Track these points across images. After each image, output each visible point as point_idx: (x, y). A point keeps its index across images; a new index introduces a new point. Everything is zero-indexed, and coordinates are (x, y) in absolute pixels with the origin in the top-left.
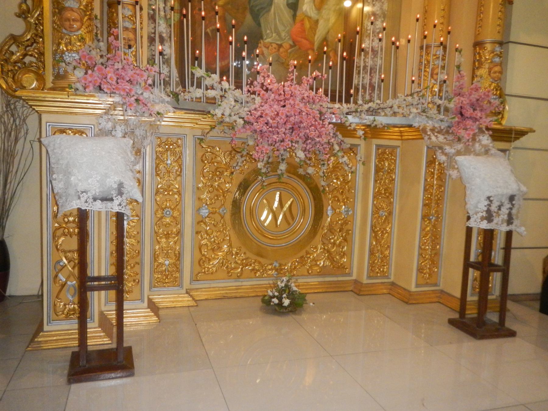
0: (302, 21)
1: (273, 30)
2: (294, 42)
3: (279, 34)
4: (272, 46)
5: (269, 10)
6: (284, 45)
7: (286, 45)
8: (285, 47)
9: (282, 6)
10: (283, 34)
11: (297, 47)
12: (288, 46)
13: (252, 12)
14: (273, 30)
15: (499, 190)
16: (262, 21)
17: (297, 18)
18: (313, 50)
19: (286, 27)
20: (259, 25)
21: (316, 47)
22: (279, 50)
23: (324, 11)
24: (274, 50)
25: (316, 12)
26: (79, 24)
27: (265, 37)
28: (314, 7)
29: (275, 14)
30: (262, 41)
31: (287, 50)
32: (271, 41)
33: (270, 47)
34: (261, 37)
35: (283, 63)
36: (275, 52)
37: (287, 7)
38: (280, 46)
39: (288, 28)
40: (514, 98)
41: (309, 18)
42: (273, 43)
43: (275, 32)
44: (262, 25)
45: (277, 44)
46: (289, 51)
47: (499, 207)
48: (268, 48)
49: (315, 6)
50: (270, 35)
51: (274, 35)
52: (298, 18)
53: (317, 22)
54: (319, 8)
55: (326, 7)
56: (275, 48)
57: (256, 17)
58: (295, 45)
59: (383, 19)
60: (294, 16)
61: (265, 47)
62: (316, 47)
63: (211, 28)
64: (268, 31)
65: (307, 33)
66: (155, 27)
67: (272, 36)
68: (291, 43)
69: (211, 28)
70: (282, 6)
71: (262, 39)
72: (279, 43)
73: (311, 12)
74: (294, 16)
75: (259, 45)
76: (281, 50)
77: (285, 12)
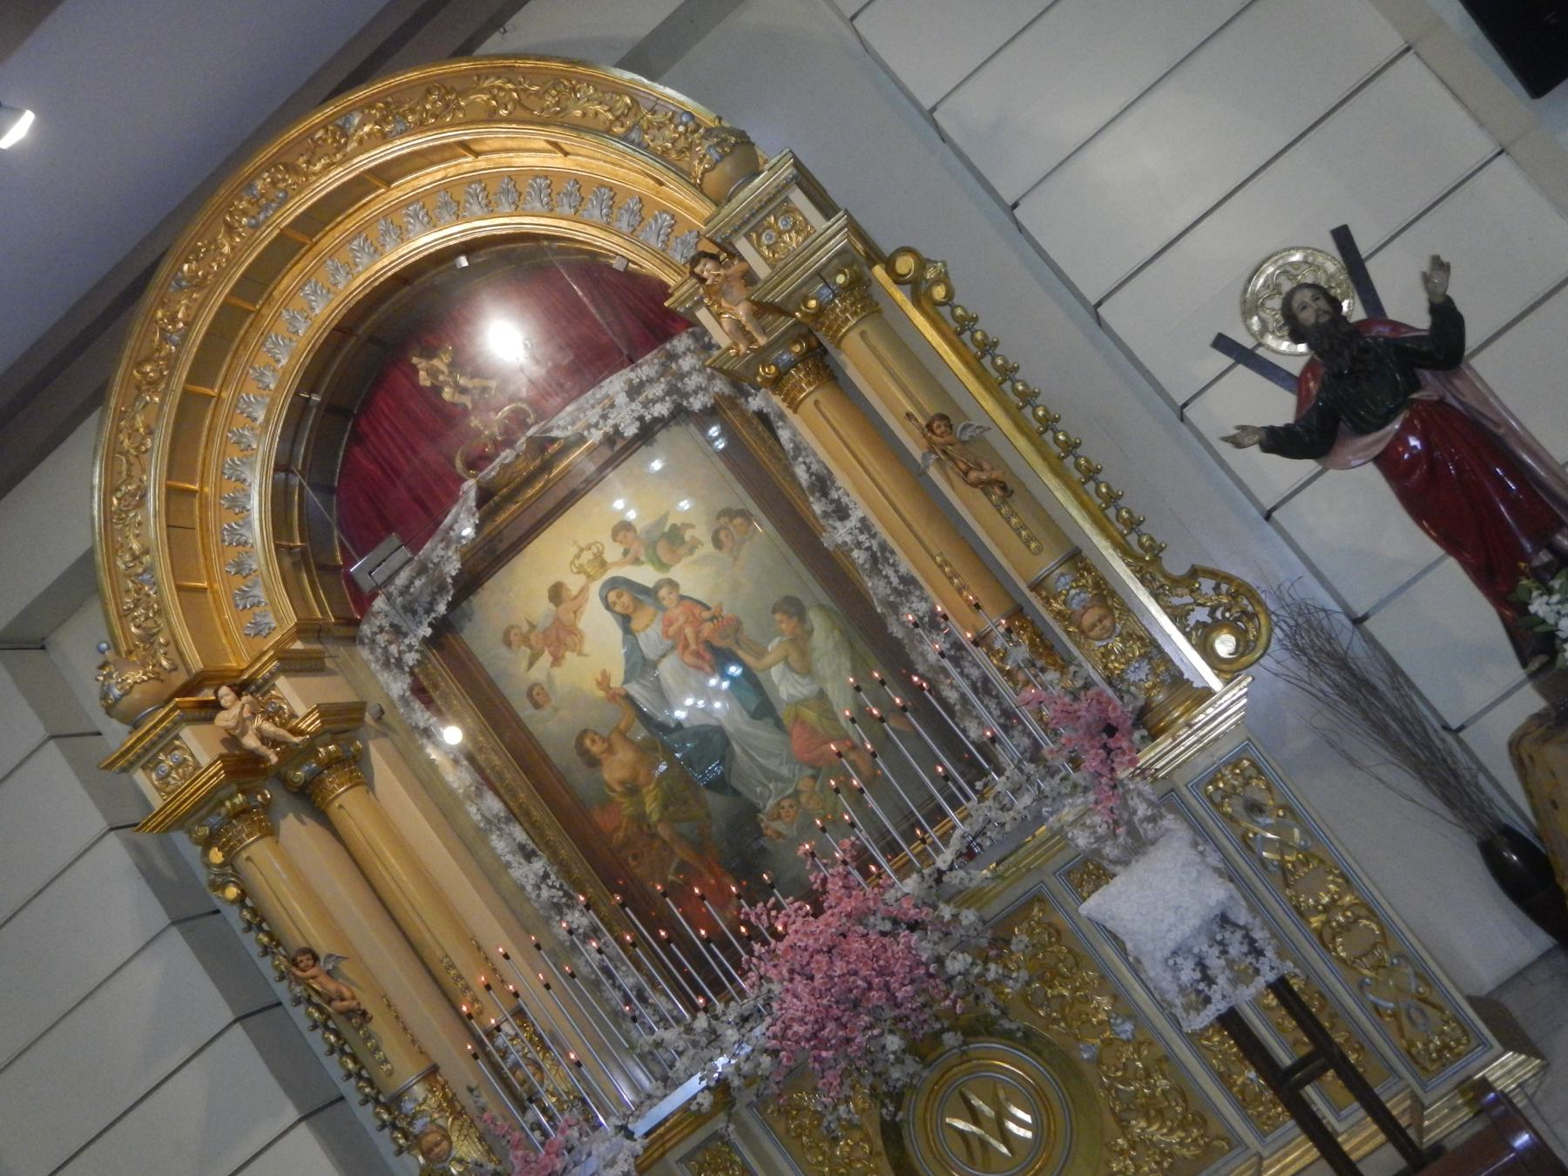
0: (797, 717)
1: (763, 780)
2: (812, 767)
3: (777, 778)
5: (733, 753)
6: (801, 786)
7: (804, 784)
10: (785, 771)
12: (810, 783)
14: (763, 780)
15: (1171, 935)
16: (735, 782)
20: (736, 793)
22: (799, 803)
25: (806, 681)
26: (445, 1144)
28: (796, 677)
30: (761, 816)
33: (783, 813)
34: (753, 811)
37: (757, 722)
39: (785, 754)
40: (1293, 500)
41: (803, 702)
43: (770, 780)
45: (788, 797)
47: (1201, 965)
48: (779, 817)
50: (767, 792)
51: (771, 786)
53: (822, 695)
54: (807, 671)
55: (816, 655)
56: (791, 806)
58: (819, 770)
59: (918, 593)
60: (778, 724)
61: (774, 820)
64: (758, 790)
65: (821, 731)
66: (587, 961)
68: (809, 772)
71: (759, 811)
72: (790, 791)
73: (799, 688)
74: (778, 724)
75: (763, 825)
76: (803, 799)
77: (760, 733)
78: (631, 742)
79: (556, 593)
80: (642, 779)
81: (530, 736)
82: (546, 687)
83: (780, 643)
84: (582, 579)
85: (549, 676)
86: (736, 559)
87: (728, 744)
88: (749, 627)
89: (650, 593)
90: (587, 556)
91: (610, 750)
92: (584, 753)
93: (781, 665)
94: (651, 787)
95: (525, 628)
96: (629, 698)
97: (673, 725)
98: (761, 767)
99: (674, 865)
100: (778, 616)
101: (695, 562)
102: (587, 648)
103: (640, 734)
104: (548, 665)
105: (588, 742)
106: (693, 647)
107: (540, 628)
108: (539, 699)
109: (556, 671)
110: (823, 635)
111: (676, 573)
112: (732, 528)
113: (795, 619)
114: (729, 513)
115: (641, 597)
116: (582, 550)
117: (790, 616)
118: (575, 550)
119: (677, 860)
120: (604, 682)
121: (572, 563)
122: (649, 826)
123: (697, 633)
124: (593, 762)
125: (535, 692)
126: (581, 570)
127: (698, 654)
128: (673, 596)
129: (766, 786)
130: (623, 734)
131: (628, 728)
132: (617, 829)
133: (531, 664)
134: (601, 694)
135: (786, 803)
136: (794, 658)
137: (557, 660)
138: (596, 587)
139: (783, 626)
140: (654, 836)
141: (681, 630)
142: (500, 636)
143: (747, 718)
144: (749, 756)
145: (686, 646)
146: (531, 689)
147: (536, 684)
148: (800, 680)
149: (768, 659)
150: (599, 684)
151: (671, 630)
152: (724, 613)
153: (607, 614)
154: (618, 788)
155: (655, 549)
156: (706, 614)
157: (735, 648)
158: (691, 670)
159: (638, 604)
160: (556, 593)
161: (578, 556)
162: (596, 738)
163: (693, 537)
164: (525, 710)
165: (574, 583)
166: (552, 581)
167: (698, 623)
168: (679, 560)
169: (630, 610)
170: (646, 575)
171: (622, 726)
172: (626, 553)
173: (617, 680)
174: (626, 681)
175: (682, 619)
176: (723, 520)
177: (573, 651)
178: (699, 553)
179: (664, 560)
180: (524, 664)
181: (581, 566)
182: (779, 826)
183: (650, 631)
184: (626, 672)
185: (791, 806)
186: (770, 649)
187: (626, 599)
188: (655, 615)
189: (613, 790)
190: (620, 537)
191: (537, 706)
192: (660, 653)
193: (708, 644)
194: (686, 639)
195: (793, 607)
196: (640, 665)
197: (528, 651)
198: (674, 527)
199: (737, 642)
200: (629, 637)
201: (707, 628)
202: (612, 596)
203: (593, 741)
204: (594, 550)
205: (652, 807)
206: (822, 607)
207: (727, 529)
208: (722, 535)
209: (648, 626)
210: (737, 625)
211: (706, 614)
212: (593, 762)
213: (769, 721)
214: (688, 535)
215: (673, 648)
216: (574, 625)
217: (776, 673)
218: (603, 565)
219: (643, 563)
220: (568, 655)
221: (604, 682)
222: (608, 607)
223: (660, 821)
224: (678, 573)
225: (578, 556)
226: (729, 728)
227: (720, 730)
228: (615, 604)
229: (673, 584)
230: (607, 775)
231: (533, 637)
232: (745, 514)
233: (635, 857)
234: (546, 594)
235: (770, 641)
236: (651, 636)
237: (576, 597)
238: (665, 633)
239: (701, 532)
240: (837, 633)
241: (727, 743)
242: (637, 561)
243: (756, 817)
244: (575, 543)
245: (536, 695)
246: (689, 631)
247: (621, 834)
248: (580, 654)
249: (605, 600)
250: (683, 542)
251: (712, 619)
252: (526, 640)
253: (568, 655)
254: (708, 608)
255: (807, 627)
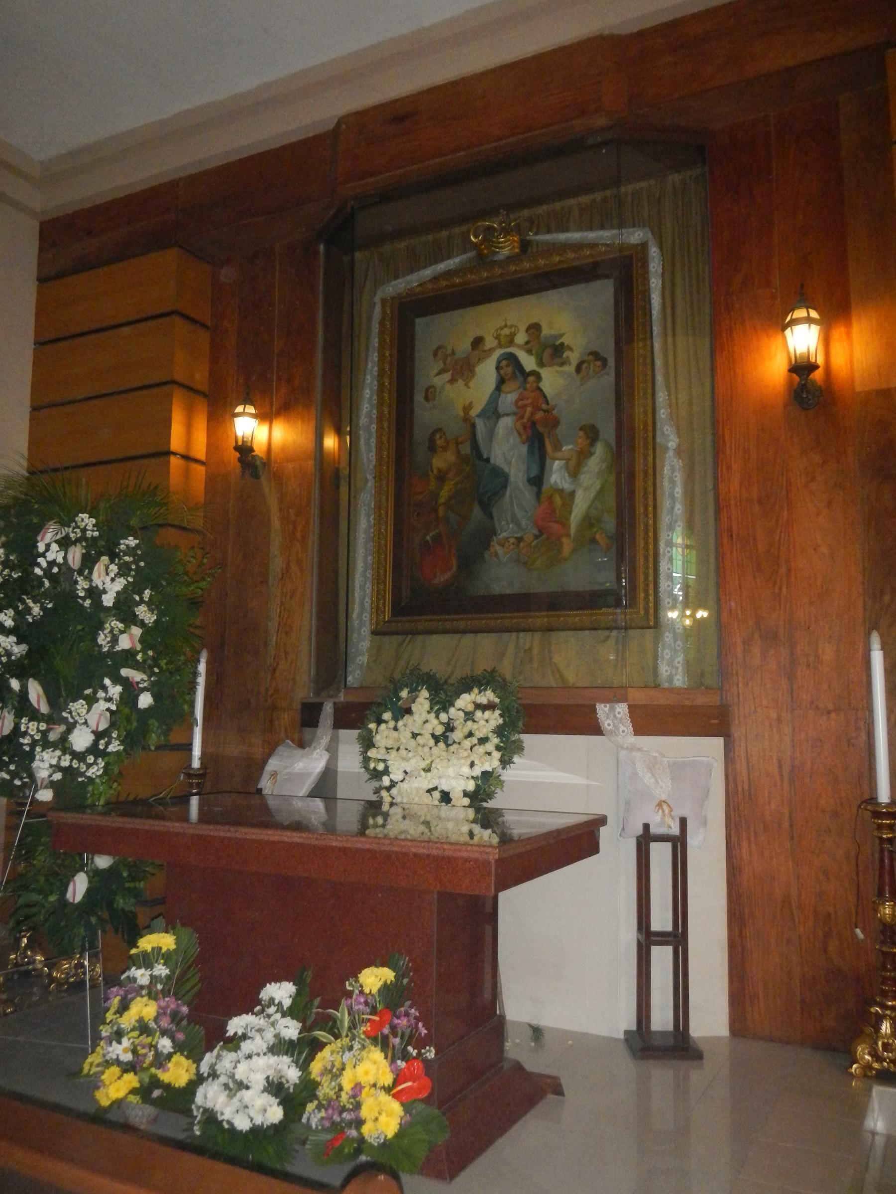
0: (550, 499)
1: (510, 521)
2: (539, 531)
3: (517, 524)
4: (508, 542)
5: (504, 495)
6: (525, 537)
7: (528, 538)
8: (527, 540)
9: (521, 485)
10: (524, 523)
11: (544, 536)
12: (532, 538)
13: (480, 502)
17: (542, 496)
18: (568, 535)
19: (526, 511)
20: (491, 517)
21: (573, 531)
22: (518, 546)
23: (583, 477)
24: (512, 547)
27: (499, 532)
28: (567, 474)
29: (511, 496)
30: (495, 538)
31: (529, 545)
32: (508, 536)
34: (494, 533)
35: (525, 564)
36: (513, 549)
38: (520, 540)
41: (561, 491)
42: (509, 537)
43: (512, 522)
44: (495, 519)
45: (517, 538)
46: (533, 544)
48: (503, 546)
49: (568, 472)
51: (511, 526)
52: (544, 496)
53: (572, 494)
54: (574, 473)
55: (586, 469)
56: (513, 544)
57: (486, 508)
60: (538, 494)
61: (499, 545)
62: (573, 531)
63: (431, 535)
64: (503, 523)
65: (558, 513)
67: (508, 527)
68: (535, 532)
69: (431, 535)
70: (521, 485)
71: (495, 534)
72: (518, 535)
73: (563, 482)
75: (492, 544)
76: (522, 544)
78: (458, 451)
79: (478, 342)
80: (450, 475)
81: (412, 412)
82: (438, 391)
83: (571, 449)
84: (496, 343)
85: (443, 387)
86: (582, 385)
87: (505, 487)
88: (561, 430)
89: (525, 375)
90: (506, 331)
91: (445, 449)
92: (432, 440)
93: (563, 462)
94: (452, 482)
95: (449, 352)
96: (473, 426)
97: (485, 456)
98: (514, 515)
99: (434, 533)
100: (581, 433)
101: (557, 372)
102: (471, 384)
103: (466, 449)
104: (447, 380)
105: (438, 436)
106: (525, 420)
107: (456, 357)
108: (430, 396)
109: (448, 387)
110: (597, 462)
111: (544, 373)
112: (592, 365)
113: (589, 441)
114: (596, 355)
115: (518, 373)
116: (506, 326)
117: (588, 437)
118: (503, 324)
119: (437, 531)
120: (467, 408)
121: (497, 330)
122: (436, 503)
123: (532, 414)
124: (432, 449)
125: (430, 390)
126: (498, 338)
127: (525, 427)
128: (535, 385)
129: (508, 523)
130: (457, 444)
131: (462, 443)
132: (421, 493)
133: (439, 373)
134: (461, 413)
135: (512, 540)
136: (573, 462)
137: (452, 381)
138: (498, 353)
139: (580, 441)
140: (435, 510)
141: (525, 406)
142: (434, 347)
143: (525, 479)
144: (512, 503)
145: (522, 417)
146: (430, 387)
147: (434, 387)
148: (567, 478)
149: (559, 455)
150: (464, 408)
151: (520, 403)
152: (554, 412)
153: (495, 371)
154: (435, 471)
155: (544, 350)
156: (544, 406)
157: (545, 436)
158: (516, 434)
159: (513, 377)
160: (478, 342)
161: (502, 328)
162: (444, 437)
163: (568, 357)
164: (419, 398)
165: (489, 342)
166: (478, 333)
167: (537, 408)
168: (551, 365)
169: (506, 378)
170: (529, 362)
171: (460, 439)
172: (527, 343)
173: (473, 413)
174: (479, 416)
175: (529, 401)
176: (591, 357)
177: (464, 380)
178: (566, 368)
179: (544, 361)
180: (435, 372)
181: (500, 335)
182: (500, 550)
183: (509, 396)
184: (482, 410)
185: (513, 544)
186: (564, 448)
187: (509, 370)
188: (519, 388)
189: (432, 472)
190: (532, 331)
191: (427, 398)
192: (508, 412)
193: (534, 424)
194: (525, 411)
195: (592, 434)
196: (492, 412)
197: (442, 366)
198: (562, 344)
199: (549, 433)
200: (497, 392)
201: (539, 415)
202: (504, 363)
203: (441, 437)
204: (513, 330)
205: (444, 494)
206: (608, 445)
207: (589, 364)
208: (584, 366)
209: (510, 392)
210: (556, 423)
211: (544, 406)
212: (432, 449)
213: (535, 489)
214: (567, 354)
215: (515, 414)
216: (474, 366)
217: (557, 464)
218: (511, 342)
219: (532, 354)
220: (460, 381)
221: (467, 408)
222: (498, 368)
223: (444, 504)
224: (544, 373)
225: (502, 328)
226: (512, 479)
227: (506, 476)
228: (502, 368)
229: (538, 377)
230: (434, 461)
231: (449, 359)
232: (604, 362)
233: (418, 515)
234: (472, 340)
235: (567, 444)
236: (509, 399)
237: (484, 351)
238: (517, 402)
239: (574, 357)
240: (604, 466)
241: (505, 486)
242: (529, 352)
243: (492, 537)
244: (506, 320)
245: (430, 394)
246: (529, 409)
247: (420, 497)
248: (466, 385)
249: (499, 362)
250: (561, 356)
251: (545, 411)
252: (445, 359)
253: (460, 381)
254: (548, 404)
255: (592, 450)
